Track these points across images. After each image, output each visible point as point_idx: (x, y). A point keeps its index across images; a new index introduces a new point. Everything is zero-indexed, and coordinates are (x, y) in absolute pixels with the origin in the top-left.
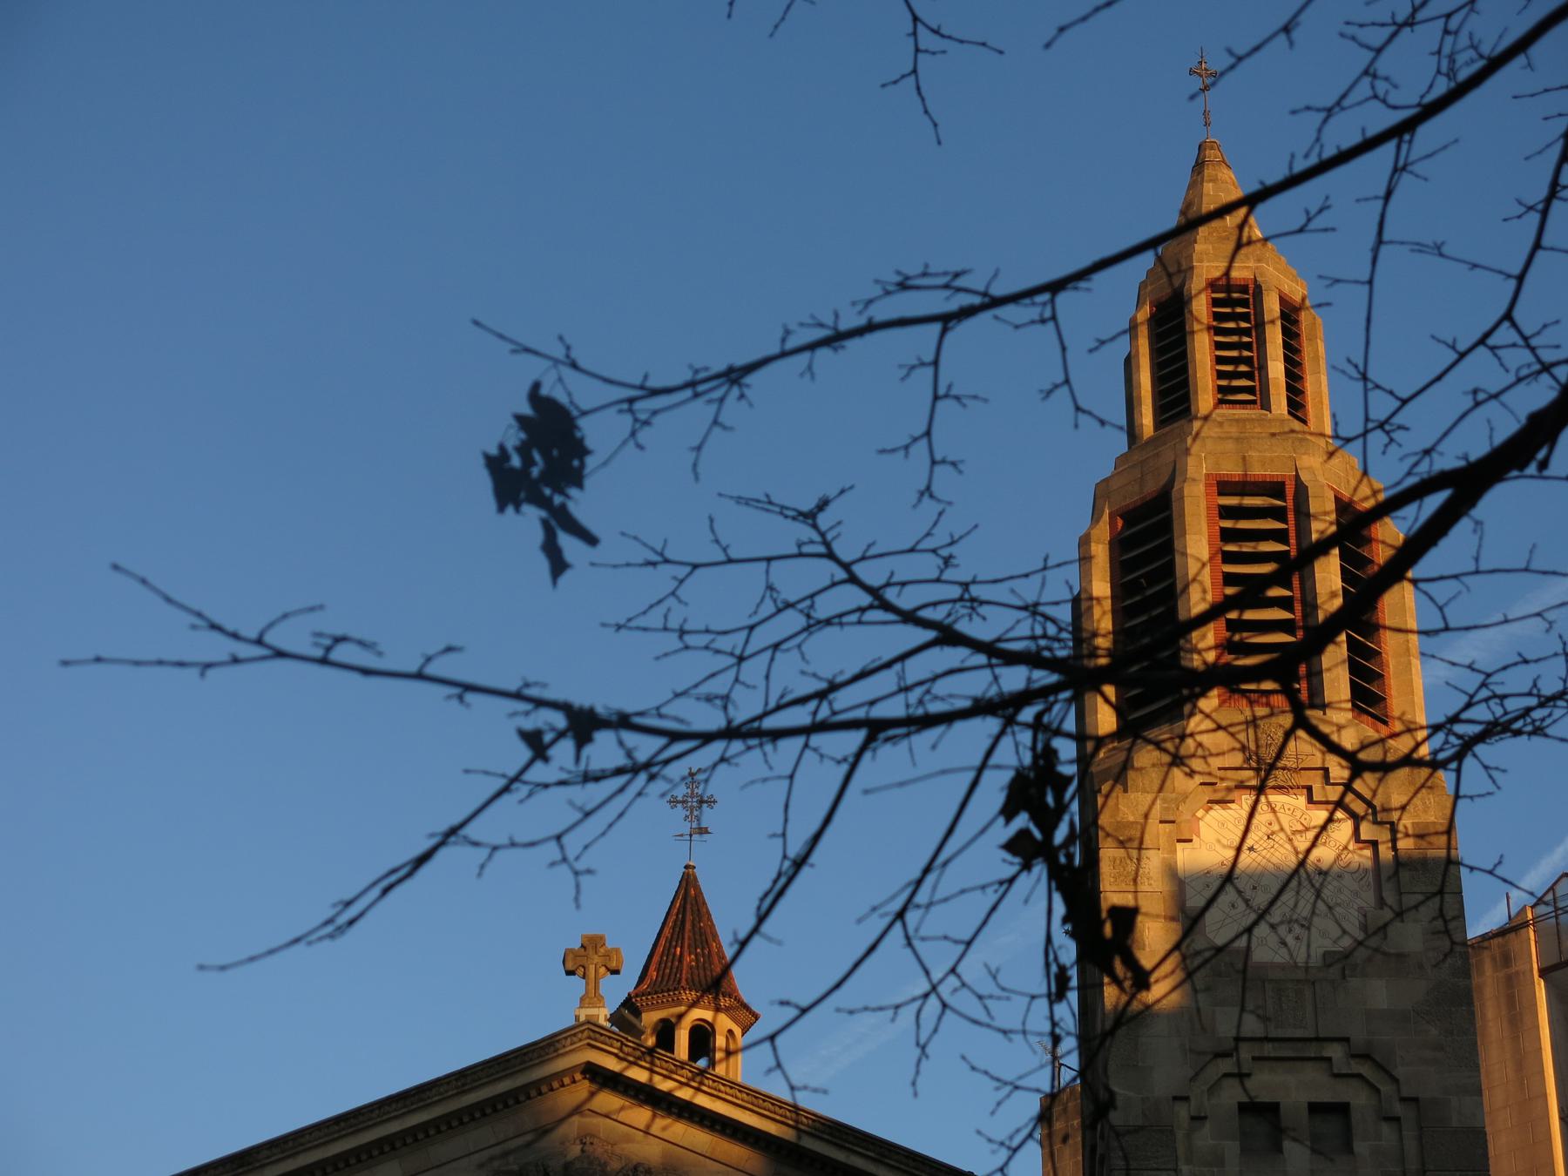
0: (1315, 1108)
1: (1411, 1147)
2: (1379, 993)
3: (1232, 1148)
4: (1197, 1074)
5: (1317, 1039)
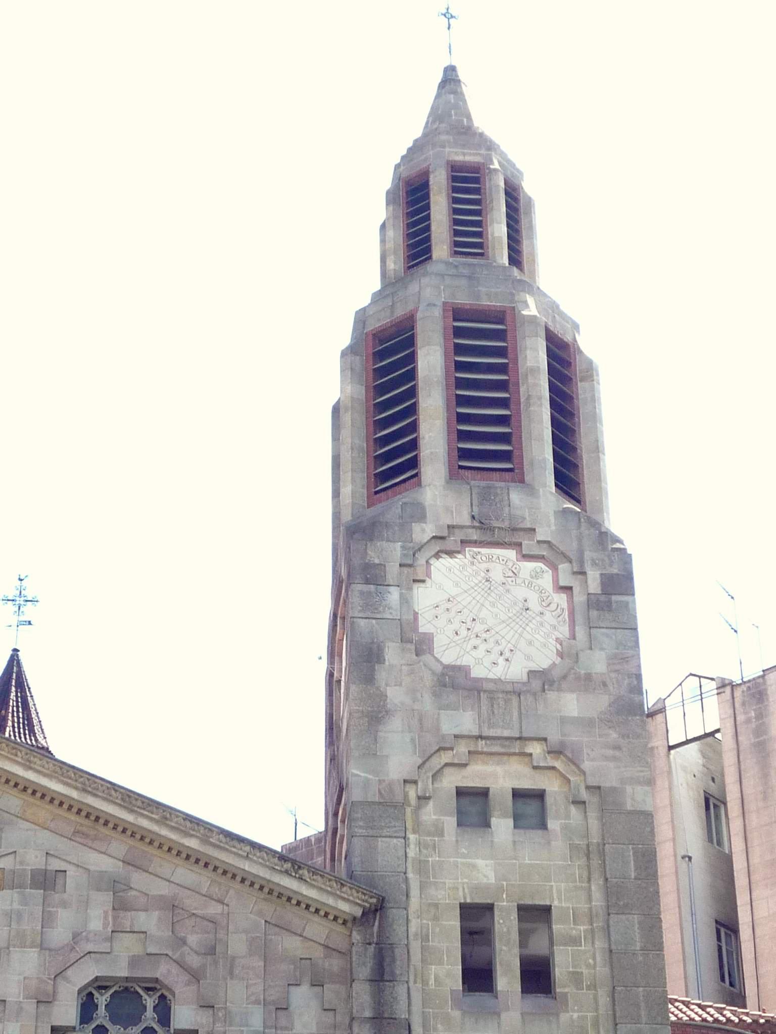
0: (518, 794)
1: (594, 824)
2: (571, 704)
3: (450, 822)
4: (424, 763)
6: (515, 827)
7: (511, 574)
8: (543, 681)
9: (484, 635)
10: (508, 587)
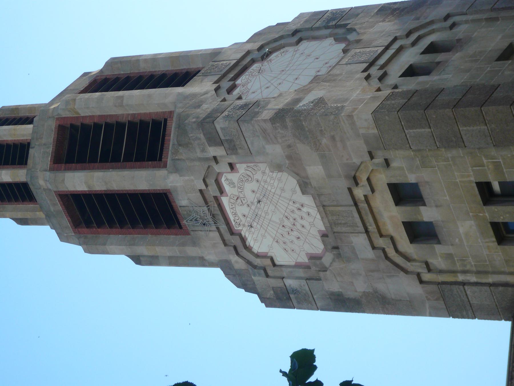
5: (356, 204)
6: (424, 204)
7: (239, 201)
8: (305, 186)
9: (291, 220)
10: (249, 203)
